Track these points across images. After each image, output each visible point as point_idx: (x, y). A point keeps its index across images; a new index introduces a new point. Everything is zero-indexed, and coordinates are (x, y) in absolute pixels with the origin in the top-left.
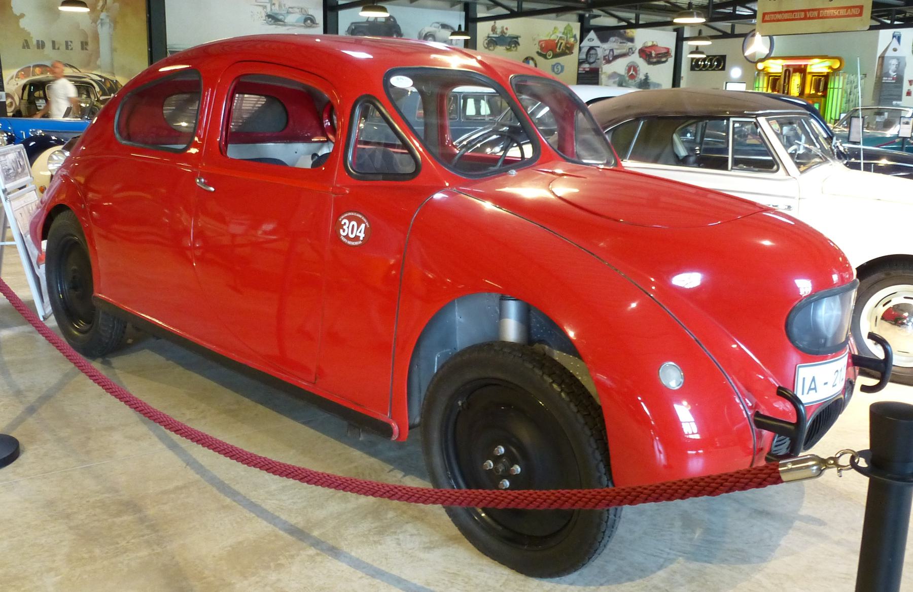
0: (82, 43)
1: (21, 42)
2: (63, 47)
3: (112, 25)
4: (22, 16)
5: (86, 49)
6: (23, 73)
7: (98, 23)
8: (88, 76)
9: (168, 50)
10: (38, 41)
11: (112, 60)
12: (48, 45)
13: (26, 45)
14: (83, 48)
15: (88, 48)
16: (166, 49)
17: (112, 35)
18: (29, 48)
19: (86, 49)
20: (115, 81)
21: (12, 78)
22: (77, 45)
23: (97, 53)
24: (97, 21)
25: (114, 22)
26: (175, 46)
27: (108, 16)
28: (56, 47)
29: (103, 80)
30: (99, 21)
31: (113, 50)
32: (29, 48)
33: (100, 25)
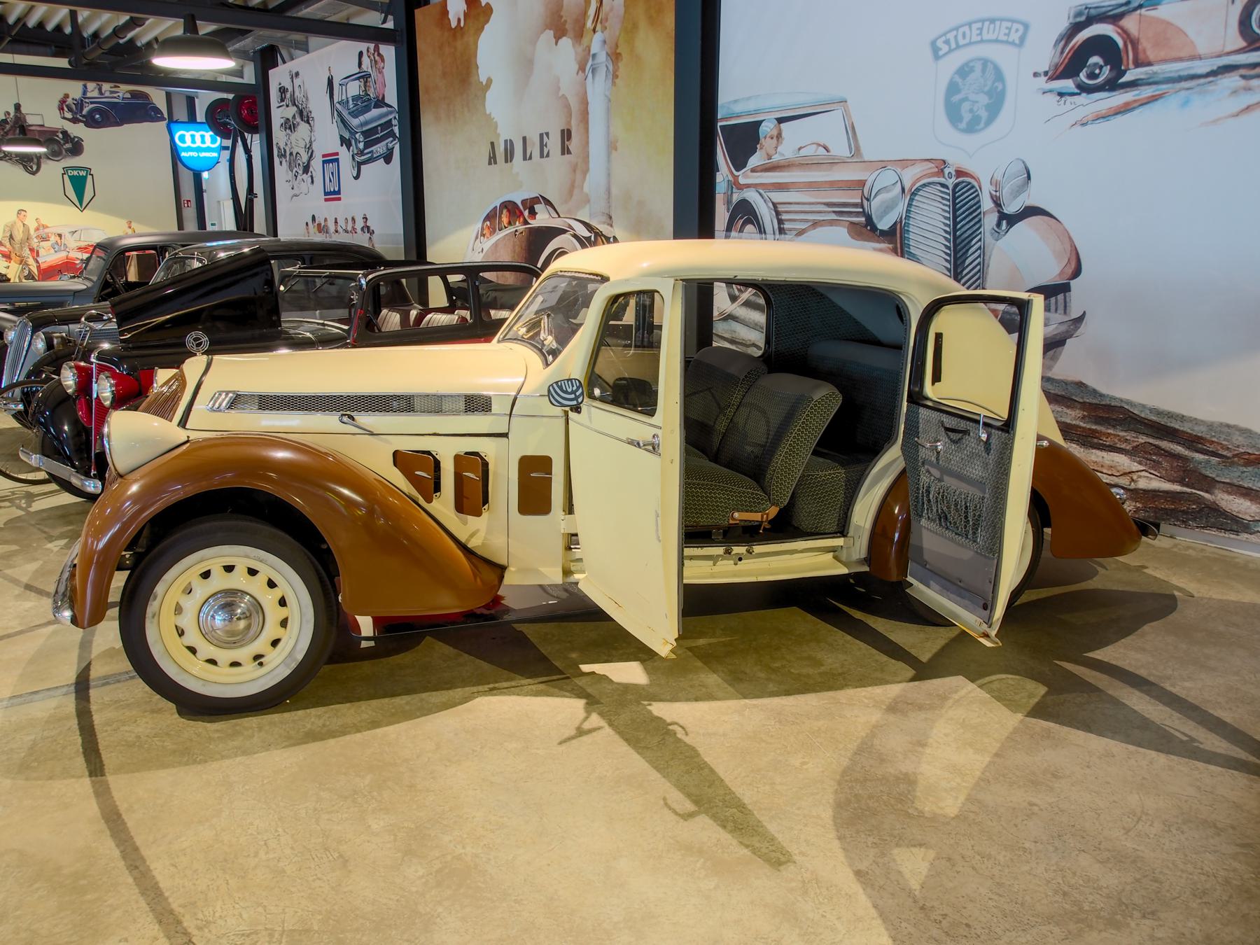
0: (563, 131)
5: (569, 152)
6: (488, 223)
8: (570, 227)
9: (719, 124)
10: (506, 141)
14: (565, 150)
17: (610, 101)
19: (569, 152)
21: (477, 238)
22: (554, 143)
29: (593, 239)
31: (612, 146)
32: (495, 163)
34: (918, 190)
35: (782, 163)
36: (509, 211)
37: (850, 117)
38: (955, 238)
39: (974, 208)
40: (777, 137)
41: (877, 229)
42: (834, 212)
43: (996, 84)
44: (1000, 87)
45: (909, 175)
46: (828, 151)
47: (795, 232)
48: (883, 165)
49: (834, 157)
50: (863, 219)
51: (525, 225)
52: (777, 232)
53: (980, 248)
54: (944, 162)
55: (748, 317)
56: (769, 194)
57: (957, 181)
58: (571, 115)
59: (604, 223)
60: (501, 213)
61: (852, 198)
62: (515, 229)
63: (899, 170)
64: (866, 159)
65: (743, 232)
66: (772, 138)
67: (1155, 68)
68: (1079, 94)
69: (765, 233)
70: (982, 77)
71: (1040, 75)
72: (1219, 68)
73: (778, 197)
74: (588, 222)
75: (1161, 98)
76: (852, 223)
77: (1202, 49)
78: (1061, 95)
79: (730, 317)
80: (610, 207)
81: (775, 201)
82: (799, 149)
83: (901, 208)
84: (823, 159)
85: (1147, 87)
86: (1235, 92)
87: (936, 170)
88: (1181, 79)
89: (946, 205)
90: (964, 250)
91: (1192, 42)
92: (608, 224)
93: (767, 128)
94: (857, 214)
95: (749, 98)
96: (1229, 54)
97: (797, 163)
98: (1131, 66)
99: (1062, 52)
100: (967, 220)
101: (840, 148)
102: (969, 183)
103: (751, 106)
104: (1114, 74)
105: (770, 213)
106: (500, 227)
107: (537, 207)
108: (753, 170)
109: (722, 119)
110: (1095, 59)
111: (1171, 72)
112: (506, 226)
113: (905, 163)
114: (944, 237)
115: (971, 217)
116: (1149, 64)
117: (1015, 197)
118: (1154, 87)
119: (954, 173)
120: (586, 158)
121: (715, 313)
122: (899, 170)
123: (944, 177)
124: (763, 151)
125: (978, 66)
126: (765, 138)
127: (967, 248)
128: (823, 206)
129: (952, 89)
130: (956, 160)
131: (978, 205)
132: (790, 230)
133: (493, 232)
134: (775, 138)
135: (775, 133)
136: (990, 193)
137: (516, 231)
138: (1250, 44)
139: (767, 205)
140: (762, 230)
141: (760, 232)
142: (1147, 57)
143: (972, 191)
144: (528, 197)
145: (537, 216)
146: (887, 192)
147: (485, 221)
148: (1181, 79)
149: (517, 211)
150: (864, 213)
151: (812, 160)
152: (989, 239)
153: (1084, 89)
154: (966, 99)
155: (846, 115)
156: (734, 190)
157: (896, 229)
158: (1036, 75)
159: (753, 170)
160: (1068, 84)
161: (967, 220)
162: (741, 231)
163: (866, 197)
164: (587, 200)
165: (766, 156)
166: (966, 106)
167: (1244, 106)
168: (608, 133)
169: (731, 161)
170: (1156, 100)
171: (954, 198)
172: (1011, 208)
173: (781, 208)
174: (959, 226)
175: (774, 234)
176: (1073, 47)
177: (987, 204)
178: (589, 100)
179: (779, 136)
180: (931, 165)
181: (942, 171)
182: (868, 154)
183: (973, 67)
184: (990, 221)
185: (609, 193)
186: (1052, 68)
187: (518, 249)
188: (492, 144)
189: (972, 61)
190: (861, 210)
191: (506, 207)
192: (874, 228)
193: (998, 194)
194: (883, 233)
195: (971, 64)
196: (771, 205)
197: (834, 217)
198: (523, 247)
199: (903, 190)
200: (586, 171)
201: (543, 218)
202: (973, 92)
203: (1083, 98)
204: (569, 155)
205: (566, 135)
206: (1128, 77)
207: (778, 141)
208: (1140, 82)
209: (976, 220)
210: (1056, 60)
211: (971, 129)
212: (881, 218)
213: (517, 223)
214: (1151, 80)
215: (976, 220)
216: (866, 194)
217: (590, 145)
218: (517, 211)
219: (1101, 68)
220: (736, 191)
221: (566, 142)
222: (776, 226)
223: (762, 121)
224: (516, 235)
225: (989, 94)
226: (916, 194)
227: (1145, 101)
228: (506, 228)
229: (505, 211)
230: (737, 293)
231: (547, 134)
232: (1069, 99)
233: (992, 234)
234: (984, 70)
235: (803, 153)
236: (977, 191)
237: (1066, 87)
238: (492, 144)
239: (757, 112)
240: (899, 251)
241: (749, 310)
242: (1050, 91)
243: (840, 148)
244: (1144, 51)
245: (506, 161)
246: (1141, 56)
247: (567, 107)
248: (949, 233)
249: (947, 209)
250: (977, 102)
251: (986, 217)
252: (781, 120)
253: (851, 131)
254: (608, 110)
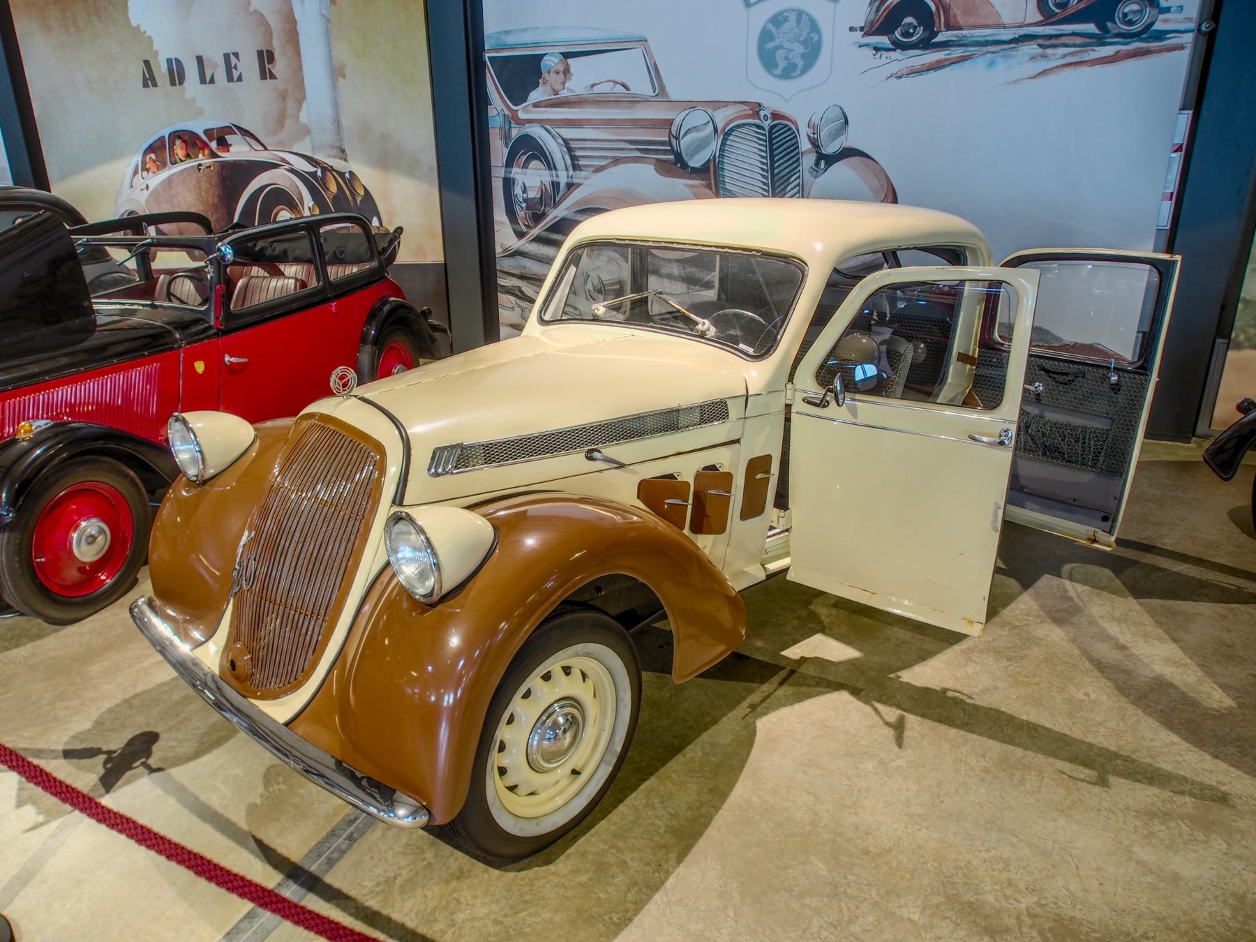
0: (260, 53)
1: (138, 71)
5: (272, 76)
6: (153, 156)
8: (284, 160)
9: (487, 55)
10: (169, 61)
12: (191, 70)
14: (266, 74)
17: (329, 21)
19: (272, 76)
20: (347, 175)
21: (136, 173)
22: (248, 65)
26: (511, 40)
29: (319, 173)
31: (336, 72)
32: (155, 85)
34: (732, 130)
35: (572, 99)
36: (184, 141)
37: (651, 57)
38: (773, 176)
39: (792, 148)
40: (564, 72)
41: (688, 166)
42: (638, 149)
43: (812, 35)
44: (816, 38)
45: (721, 117)
46: (627, 89)
47: (593, 169)
48: (692, 105)
49: (635, 96)
50: (672, 157)
51: (214, 158)
52: (571, 169)
53: (799, 185)
54: (759, 105)
55: (540, 252)
56: (557, 130)
57: (773, 123)
58: (271, 35)
59: (334, 157)
60: (172, 144)
61: (658, 137)
62: (197, 163)
63: (710, 111)
64: (672, 99)
65: (527, 168)
66: (558, 73)
67: (964, 32)
68: (895, 50)
69: (556, 169)
70: (797, 27)
71: (856, 30)
72: (1020, 36)
73: (568, 133)
74: (309, 154)
75: (970, 58)
76: (659, 160)
77: (1006, 19)
78: (877, 49)
79: (518, 253)
80: (340, 139)
81: (565, 137)
82: (593, 86)
83: (714, 147)
84: (622, 97)
85: (957, 48)
86: (1033, 58)
87: (751, 112)
88: (987, 43)
89: (763, 145)
90: (783, 187)
91: (998, 13)
92: (341, 159)
93: (551, 62)
94: (665, 152)
95: (525, 30)
96: (1029, 25)
97: (590, 99)
98: (943, 28)
99: (877, 11)
100: (785, 159)
101: (641, 86)
102: (786, 126)
103: (528, 38)
104: (927, 34)
105: (561, 150)
106: (173, 159)
107: (229, 138)
108: (536, 105)
109: (490, 50)
110: (909, 20)
111: (978, 36)
112: (183, 159)
113: (717, 105)
114: (761, 175)
115: (789, 157)
116: (960, 28)
117: (833, 140)
118: (964, 49)
119: (769, 116)
120: (300, 85)
121: (498, 250)
122: (710, 111)
123: (759, 119)
124: (548, 86)
125: (793, 17)
126: (549, 72)
127: (785, 184)
128: (624, 143)
129: (765, 36)
130: (772, 103)
131: (796, 146)
132: (587, 166)
133: (162, 165)
134: (561, 73)
135: (561, 68)
136: (808, 135)
137: (200, 165)
138: (1046, 19)
139: (556, 141)
140: (552, 166)
141: (550, 168)
142: (958, 22)
143: (789, 133)
144: (214, 127)
145: (231, 149)
146: (698, 132)
147: (146, 153)
148: (987, 43)
149: (198, 142)
150: (672, 151)
151: (608, 97)
152: (807, 176)
153: (898, 46)
154: (780, 47)
155: (647, 54)
156: (513, 125)
157: (709, 167)
158: (852, 29)
159: (536, 105)
160: (884, 40)
161: (785, 159)
162: (525, 166)
163: (674, 135)
164: (306, 131)
165: (551, 91)
166: (780, 55)
167: (1041, 70)
168: (330, 57)
169: (510, 101)
170: (966, 60)
171: (771, 139)
172: (831, 149)
173: (573, 145)
174: (776, 165)
175: (567, 169)
176: (888, 6)
177: (805, 145)
178: (297, 20)
179: (567, 71)
180: (745, 107)
181: (758, 113)
182: (674, 93)
183: (788, 17)
184: (808, 161)
185: (338, 123)
186: (867, 25)
187: (204, 186)
188: (147, 63)
189: (786, 11)
190: (669, 148)
191: (180, 137)
192: (684, 166)
193: (816, 136)
194: (694, 170)
195: (785, 14)
196: (560, 141)
197: (639, 154)
198: (214, 182)
199: (716, 130)
200: (301, 99)
201: (239, 151)
202: (788, 41)
203: (897, 54)
204: (273, 81)
205: (266, 58)
206: (940, 38)
207: (565, 76)
208: (951, 43)
209: (794, 159)
210: (872, 17)
211: (788, 73)
212: (692, 156)
213: (201, 156)
214: (961, 42)
215: (794, 159)
216: (674, 134)
217: (305, 69)
218: (198, 142)
219: (915, 28)
220: (516, 126)
221: (267, 66)
222: (569, 162)
223: (545, 55)
224: (200, 170)
225: (805, 43)
226: (730, 134)
227: (955, 60)
228: (182, 161)
229: (178, 142)
230: (524, 229)
231: (236, 55)
232: (885, 54)
233: (810, 173)
234: (799, 21)
235: (596, 89)
236: (794, 132)
237: (882, 43)
238: (147, 63)
239: (536, 45)
240: (713, 187)
241: (542, 246)
242: (867, 45)
243: (641, 86)
244: (955, 17)
245: (173, 83)
246: (952, 20)
247: (265, 24)
248: (767, 171)
249: (764, 148)
250: (793, 50)
251: (805, 156)
252: (567, 55)
253: (654, 72)
254: (328, 33)
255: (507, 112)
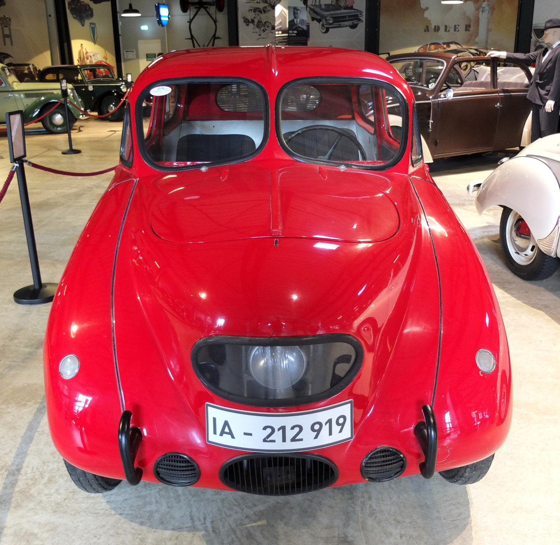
0: (466, 26)
1: (424, 28)
2: (452, 30)
3: (491, 11)
4: (427, 9)
5: (469, 30)
6: (422, 49)
7: (480, 10)
9: (533, 28)
10: (435, 26)
11: (487, 38)
12: (442, 29)
13: (427, 29)
14: (466, 30)
15: (470, 29)
16: (532, 27)
18: (428, 31)
19: (469, 30)
22: (462, 28)
23: (477, 34)
24: (479, 9)
25: (492, 9)
26: (539, 25)
27: (488, 5)
28: (448, 30)
29: (478, 53)
30: (481, 9)
31: (489, 30)
32: (428, 31)
33: (481, 12)
109: (534, 27)
255: (536, 40)
